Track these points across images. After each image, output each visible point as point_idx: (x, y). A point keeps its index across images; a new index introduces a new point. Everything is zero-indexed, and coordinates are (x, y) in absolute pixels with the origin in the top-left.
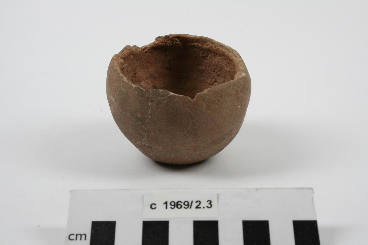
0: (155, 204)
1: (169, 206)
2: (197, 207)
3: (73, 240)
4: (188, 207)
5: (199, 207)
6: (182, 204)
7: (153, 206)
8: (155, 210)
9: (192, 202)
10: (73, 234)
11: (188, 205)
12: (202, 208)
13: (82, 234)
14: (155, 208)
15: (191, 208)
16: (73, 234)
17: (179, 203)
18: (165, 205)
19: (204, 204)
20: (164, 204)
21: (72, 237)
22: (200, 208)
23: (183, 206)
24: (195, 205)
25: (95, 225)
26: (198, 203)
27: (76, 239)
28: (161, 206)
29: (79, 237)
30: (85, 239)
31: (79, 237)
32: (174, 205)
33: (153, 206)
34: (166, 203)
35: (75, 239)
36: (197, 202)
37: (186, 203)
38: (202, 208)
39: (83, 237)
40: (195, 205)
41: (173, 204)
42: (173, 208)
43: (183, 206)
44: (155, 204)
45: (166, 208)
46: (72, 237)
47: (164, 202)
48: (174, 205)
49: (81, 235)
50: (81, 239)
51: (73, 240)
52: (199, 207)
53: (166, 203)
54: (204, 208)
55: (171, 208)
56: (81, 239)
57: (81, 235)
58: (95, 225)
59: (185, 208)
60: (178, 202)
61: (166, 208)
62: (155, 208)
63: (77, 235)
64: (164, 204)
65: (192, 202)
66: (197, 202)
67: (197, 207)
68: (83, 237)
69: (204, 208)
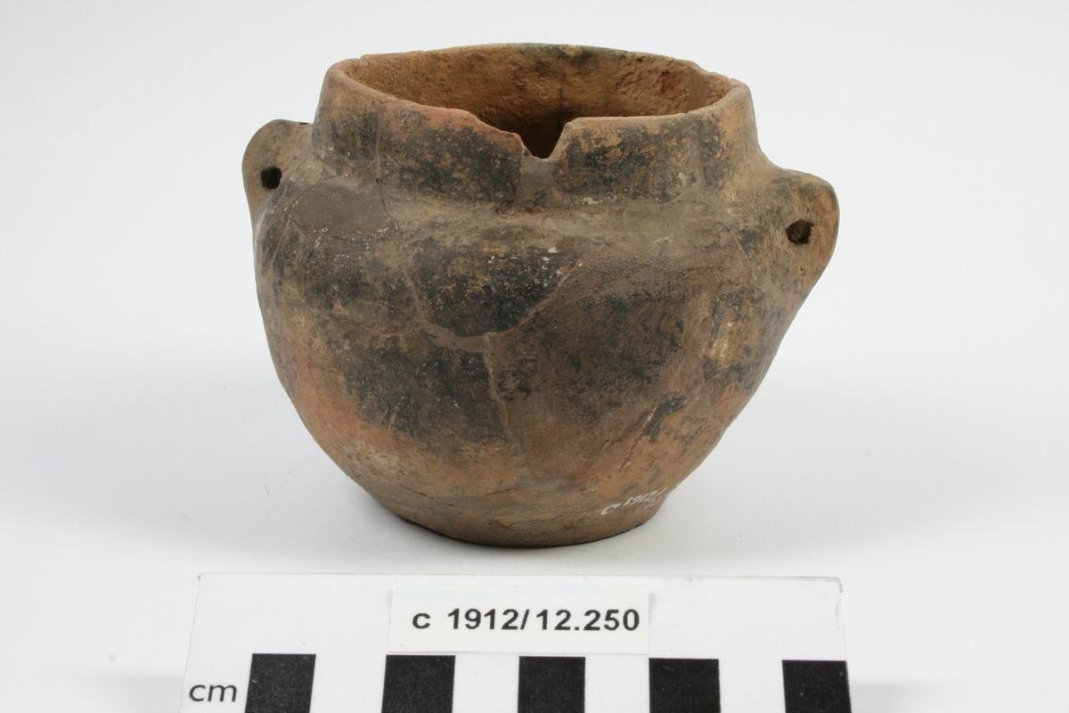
0: (427, 616)
1: (462, 621)
2: (559, 627)
3: (202, 700)
5: (593, 626)
7: (421, 621)
8: (425, 630)
10: (203, 687)
13: (225, 686)
16: (203, 687)
18: (453, 617)
19: (579, 619)
21: (198, 693)
22: (568, 628)
25: (262, 664)
26: (564, 616)
27: (210, 699)
28: (440, 622)
29: (217, 692)
30: (234, 699)
31: (217, 692)
33: (421, 621)
34: (456, 613)
36: (559, 613)
39: (229, 693)
42: (473, 628)
44: (427, 616)
45: (456, 626)
46: (198, 693)
49: (223, 689)
50: (222, 699)
51: (202, 700)
52: (593, 626)
53: (456, 613)
54: (577, 629)
55: (468, 626)
56: (222, 699)
57: (223, 689)
58: (262, 664)
61: (456, 626)
66: (559, 613)
67: (559, 627)
68: (229, 693)
69: (577, 629)
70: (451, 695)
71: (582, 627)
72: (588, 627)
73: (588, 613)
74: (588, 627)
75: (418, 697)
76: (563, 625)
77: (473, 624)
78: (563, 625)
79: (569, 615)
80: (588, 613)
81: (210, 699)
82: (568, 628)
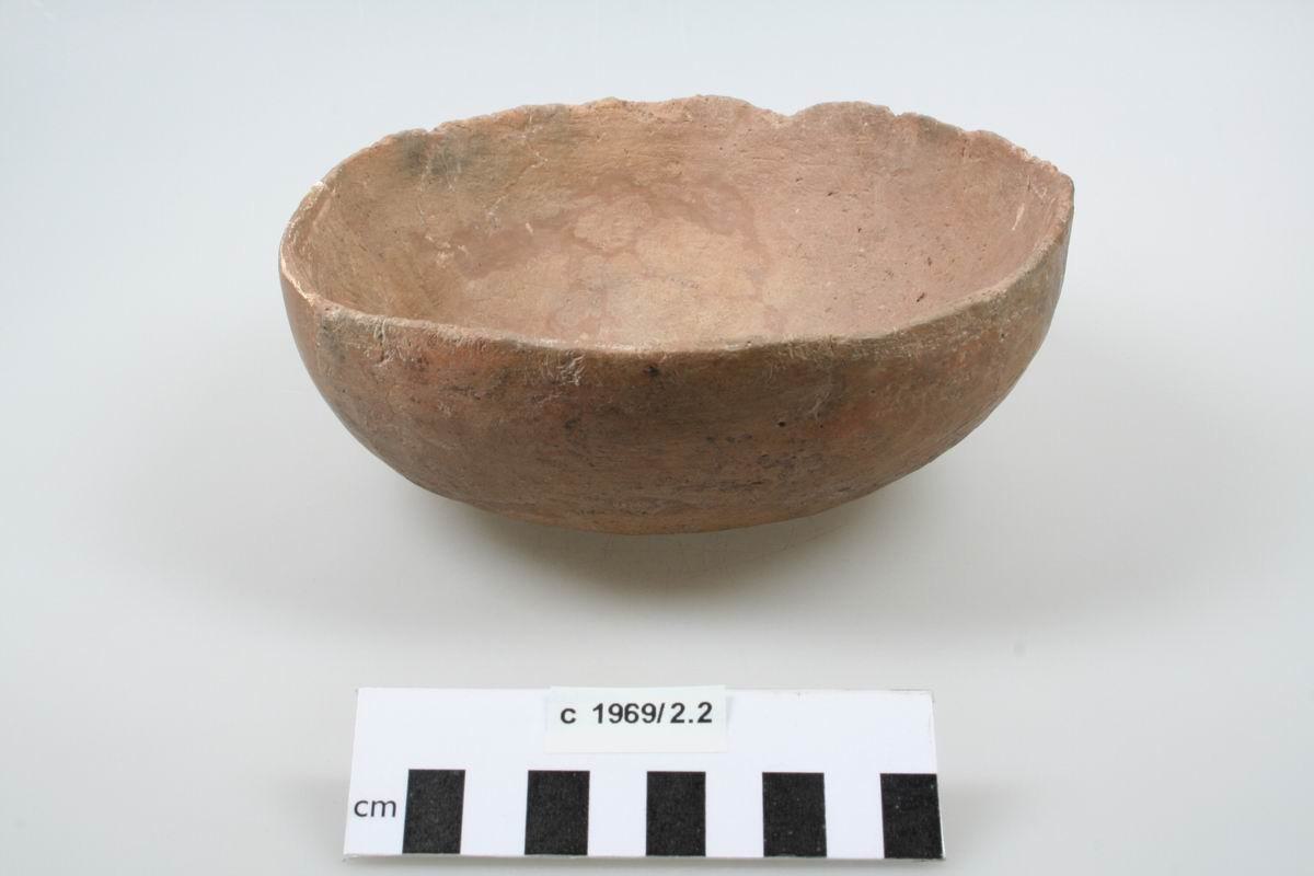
0: (573, 711)
2: (674, 720)
3: (365, 815)
4: (653, 720)
6: (639, 712)
7: (568, 716)
9: (663, 706)
10: (366, 802)
11: (653, 714)
12: (687, 721)
13: (385, 801)
14: (573, 720)
15: (659, 721)
16: (366, 802)
17: (632, 709)
18: (597, 712)
20: (595, 710)
21: (363, 809)
22: (682, 721)
23: (641, 716)
24: (669, 713)
25: (418, 780)
26: (678, 708)
27: (373, 815)
28: (586, 715)
29: (379, 808)
30: (394, 814)
31: (379, 808)
32: (620, 714)
34: (600, 708)
35: (369, 814)
36: (674, 706)
37: (649, 710)
38: (687, 721)
39: (389, 808)
40: (669, 713)
41: (616, 710)
43: (641, 716)
44: (573, 711)
45: (600, 721)
47: (596, 706)
48: (620, 714)
49: (384, 805)
50: (383, 814)
51: (365, 815)
53: (600, 708)
54: (691, 721)
55: (612, 721)
56: (383, 814)
57: (384, 805)
58: (418, 780)
59: (645, 720)
60: (629, 706)
61: (600, 721)
62: (573, 720)
63: (374, 803)
64: (595, 710)
65: (663, 706)
66: (674, 706)
67: (674, 720)
68: (389, 808)
69: (691, 721)
70: (587, 809)
71: (696, 718)
72: (701, 720)
73: (701, 706)
74: (701, 720)
75: (558, 812)
76: (678, 718)
77: (616, 718)
78: (678, 718)
79: (683, 708)
80: (701, 706)
81: (373, 815)
82: (682, 721)
